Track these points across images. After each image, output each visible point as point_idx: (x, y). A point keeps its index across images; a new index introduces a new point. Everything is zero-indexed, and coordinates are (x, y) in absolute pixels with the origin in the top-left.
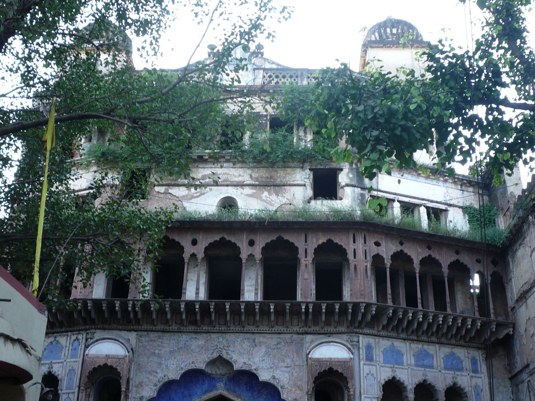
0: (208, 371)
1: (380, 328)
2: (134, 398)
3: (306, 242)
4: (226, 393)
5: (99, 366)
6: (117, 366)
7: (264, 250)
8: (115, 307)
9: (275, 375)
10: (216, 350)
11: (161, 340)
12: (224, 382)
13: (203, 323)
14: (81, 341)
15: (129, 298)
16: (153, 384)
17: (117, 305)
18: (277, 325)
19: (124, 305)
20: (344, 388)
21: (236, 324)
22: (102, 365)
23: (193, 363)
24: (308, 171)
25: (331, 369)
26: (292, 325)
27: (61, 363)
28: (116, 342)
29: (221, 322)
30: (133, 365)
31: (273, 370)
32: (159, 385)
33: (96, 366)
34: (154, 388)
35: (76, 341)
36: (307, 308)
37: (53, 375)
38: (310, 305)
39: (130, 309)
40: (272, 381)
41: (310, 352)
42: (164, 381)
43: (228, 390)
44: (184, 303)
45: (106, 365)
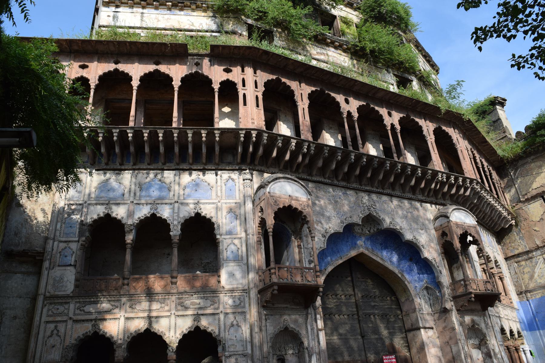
2: (306, 248)
4: (366, 252)
12: (363, 240)
14: (237, 181)
24: (392, 75)
27: (214, 203)
34: (323, 239)
35: (230, 181)
37: (204, 217)
40: (414, 241)
43: (367, 249)
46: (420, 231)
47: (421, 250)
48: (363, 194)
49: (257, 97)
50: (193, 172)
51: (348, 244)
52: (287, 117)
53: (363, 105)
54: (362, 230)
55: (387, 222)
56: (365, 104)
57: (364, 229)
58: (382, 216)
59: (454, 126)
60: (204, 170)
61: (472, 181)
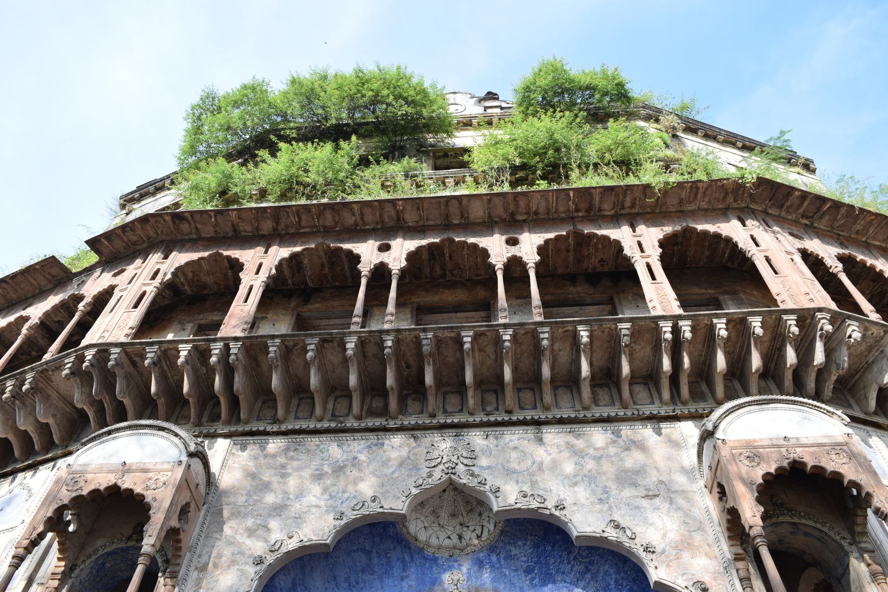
0: (419, 530)
1: (872, 404)
3: (634, 231)
5: (95, 492)
6: (147, 488)
7: (541, 250)
8: (179, 357)
9: (616, 517)
10: (441, 467)
11: (292, 454)
13: (403, 410)
15: (219, 335)
16: (251, 561)
17: (183, 354)
18: (597, 405)
19: (201, 354)
20: (845, 544)
21: (489, 409)
22: (102, 488)
23: (374, 501)
25: (797, 466)
26: (635, 403)
28: (161, 433)
29: (449, 410)
30: (203, 512)
31: (610, 508)
32: (270, 559)
33: (85, 492)
36: (676, 331)
38: (681, 323)
39: (213, 359)
40: (612, 534)
41: (716, 427)
42: (284, 550)
44: (354, 339)
45: (114, 490)
46: (645, 503)
47: (643, 564)
48: (436, 437)
49: (144, 293)
50: (21, 475)
51: (404, 584)
52: (277, 325)
53: (430, 245)
54: (460, 537)
55: (510, 496)
56: (437, 240)
57: (467, 535)
58: (492, 481)
59: (724, 214)
60: (34, 467)
61: (806, 318)
